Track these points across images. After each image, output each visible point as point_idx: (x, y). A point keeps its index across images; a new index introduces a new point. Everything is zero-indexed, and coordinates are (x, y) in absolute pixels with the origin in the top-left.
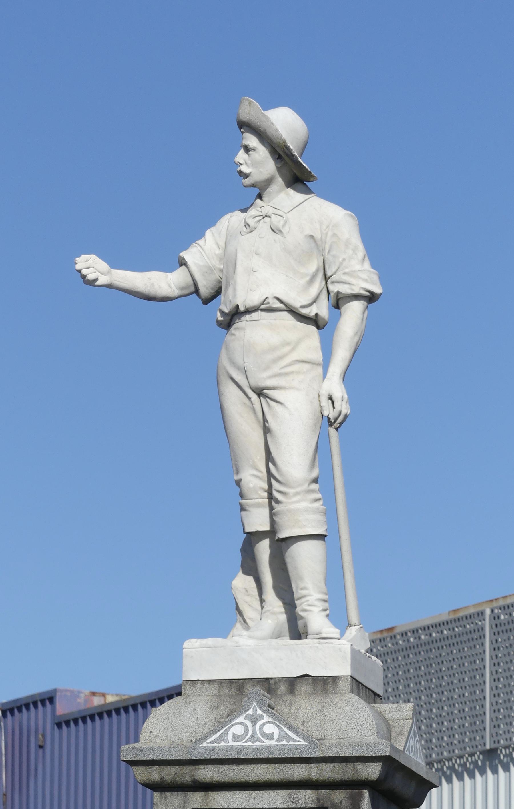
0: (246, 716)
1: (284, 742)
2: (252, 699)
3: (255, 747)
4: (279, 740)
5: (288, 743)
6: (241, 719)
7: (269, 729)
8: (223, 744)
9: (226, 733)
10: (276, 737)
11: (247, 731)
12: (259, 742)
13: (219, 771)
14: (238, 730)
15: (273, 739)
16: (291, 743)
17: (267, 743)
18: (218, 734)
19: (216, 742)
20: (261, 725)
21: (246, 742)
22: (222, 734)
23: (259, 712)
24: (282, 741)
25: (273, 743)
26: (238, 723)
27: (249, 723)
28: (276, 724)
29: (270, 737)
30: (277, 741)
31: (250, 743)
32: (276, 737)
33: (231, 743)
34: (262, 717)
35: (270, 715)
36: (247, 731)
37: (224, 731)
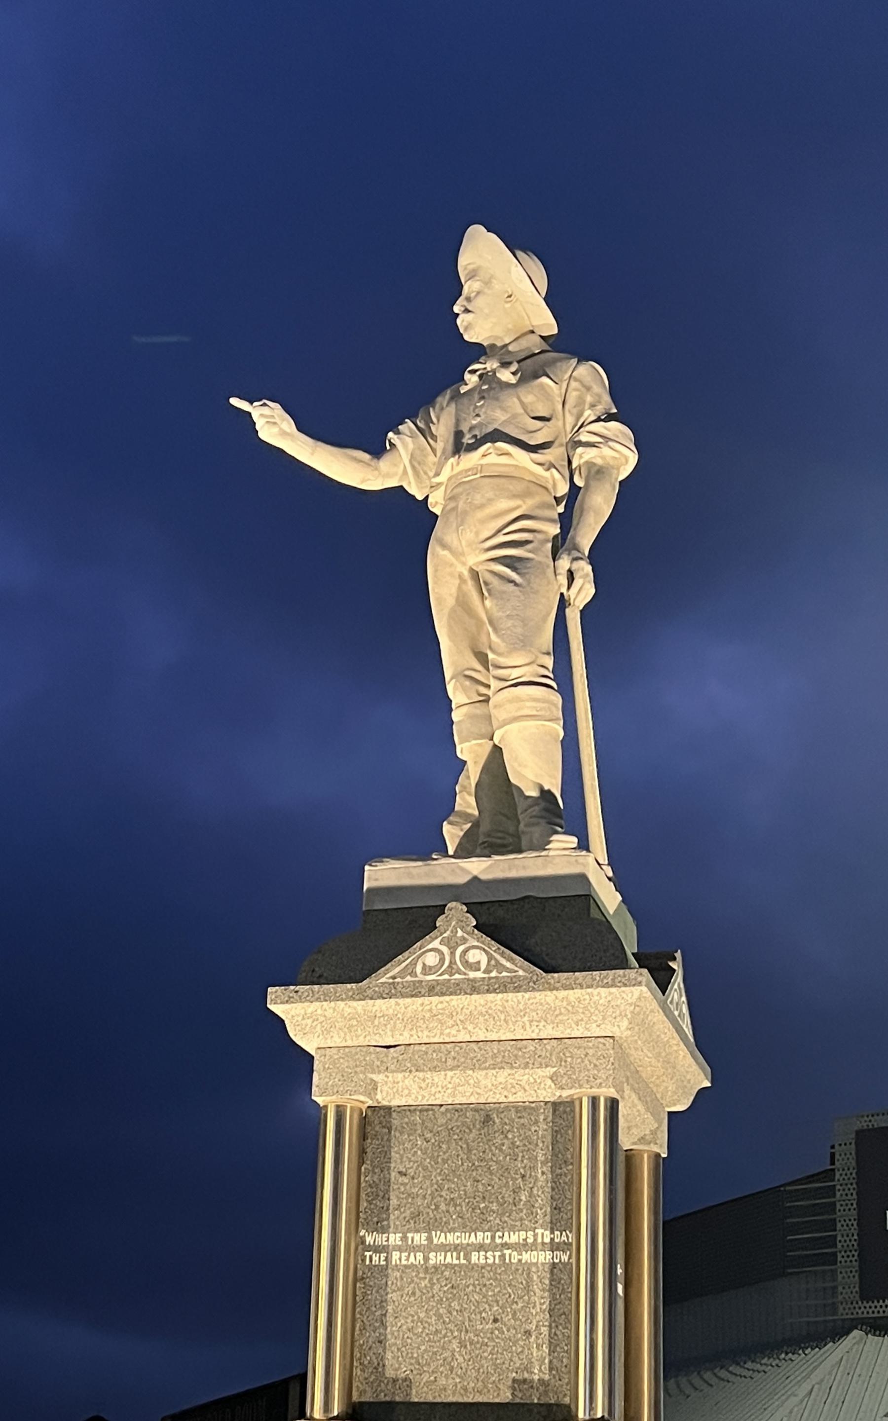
0: (442, 941)
1: (494, 974)
2: (450, 916)
3: (453, 981)
4: (487, 971)
5: (500, 973)
6: (436, 944)
7: (475, 956)
8: (409, 978)
9: (414, 964)
10: (483, 966)
11: (442, 960)
12: (459, 974)
13: (403, 1019)
14: (431, 959)
15: (479, 970)
16: (504, 974)
17: (472, 975)
18: (404, 965)
19: (400, 977)
20: (463, 951)
21: (440, 975)
22: (407, 965)
23: (460, 933)
24: (491, 971)
25: (479, 975)
26: (431, 950)
27: (445, 949)
28: (484, 950)
29: (476, 967)
30: (484, 972)
31: (446, 977)
32: (483, 966)
33: (421, 977)
34: (464, 940)
35: (475, 937)
36: (442, 960)
37: (411, 962)
